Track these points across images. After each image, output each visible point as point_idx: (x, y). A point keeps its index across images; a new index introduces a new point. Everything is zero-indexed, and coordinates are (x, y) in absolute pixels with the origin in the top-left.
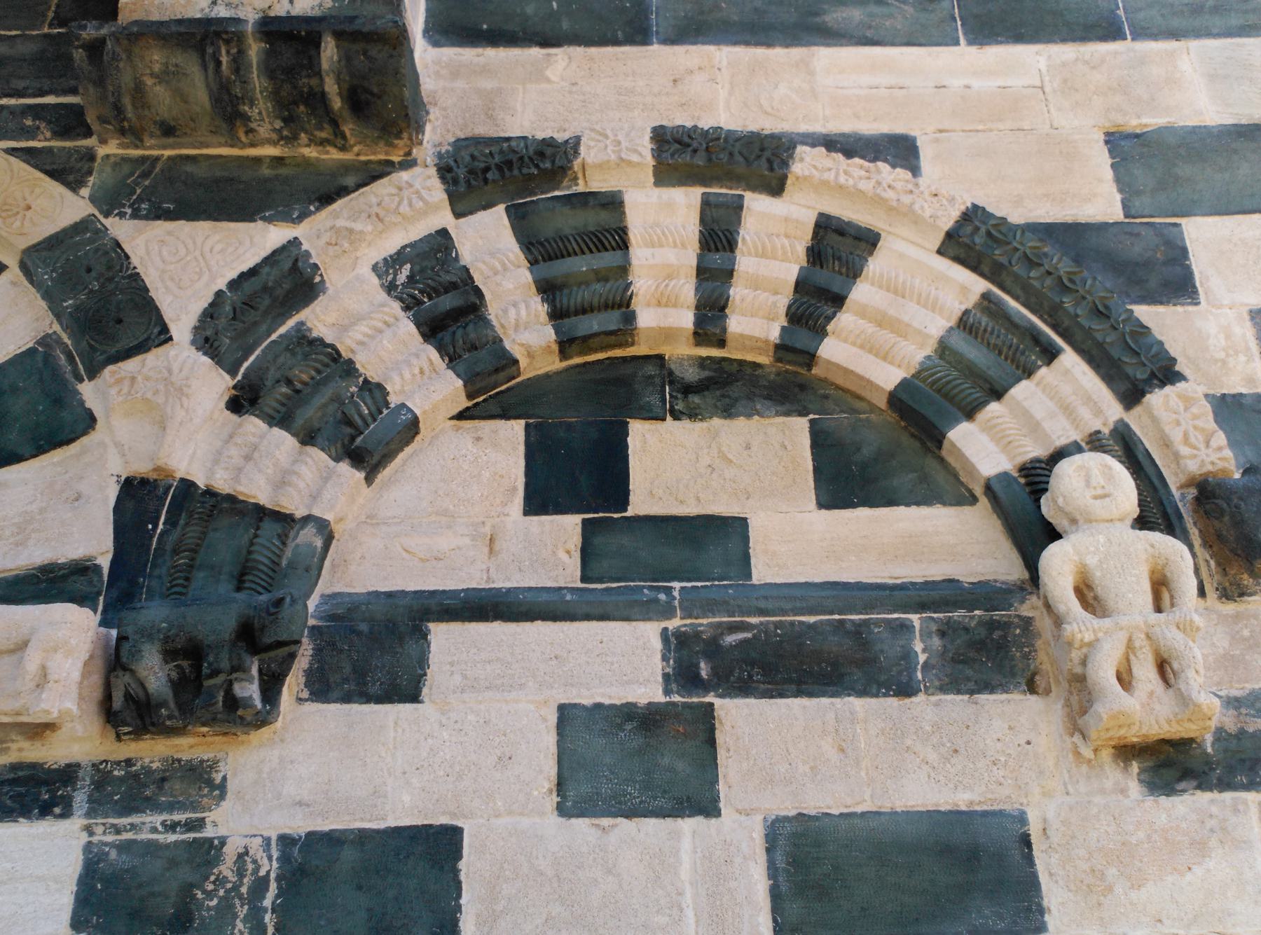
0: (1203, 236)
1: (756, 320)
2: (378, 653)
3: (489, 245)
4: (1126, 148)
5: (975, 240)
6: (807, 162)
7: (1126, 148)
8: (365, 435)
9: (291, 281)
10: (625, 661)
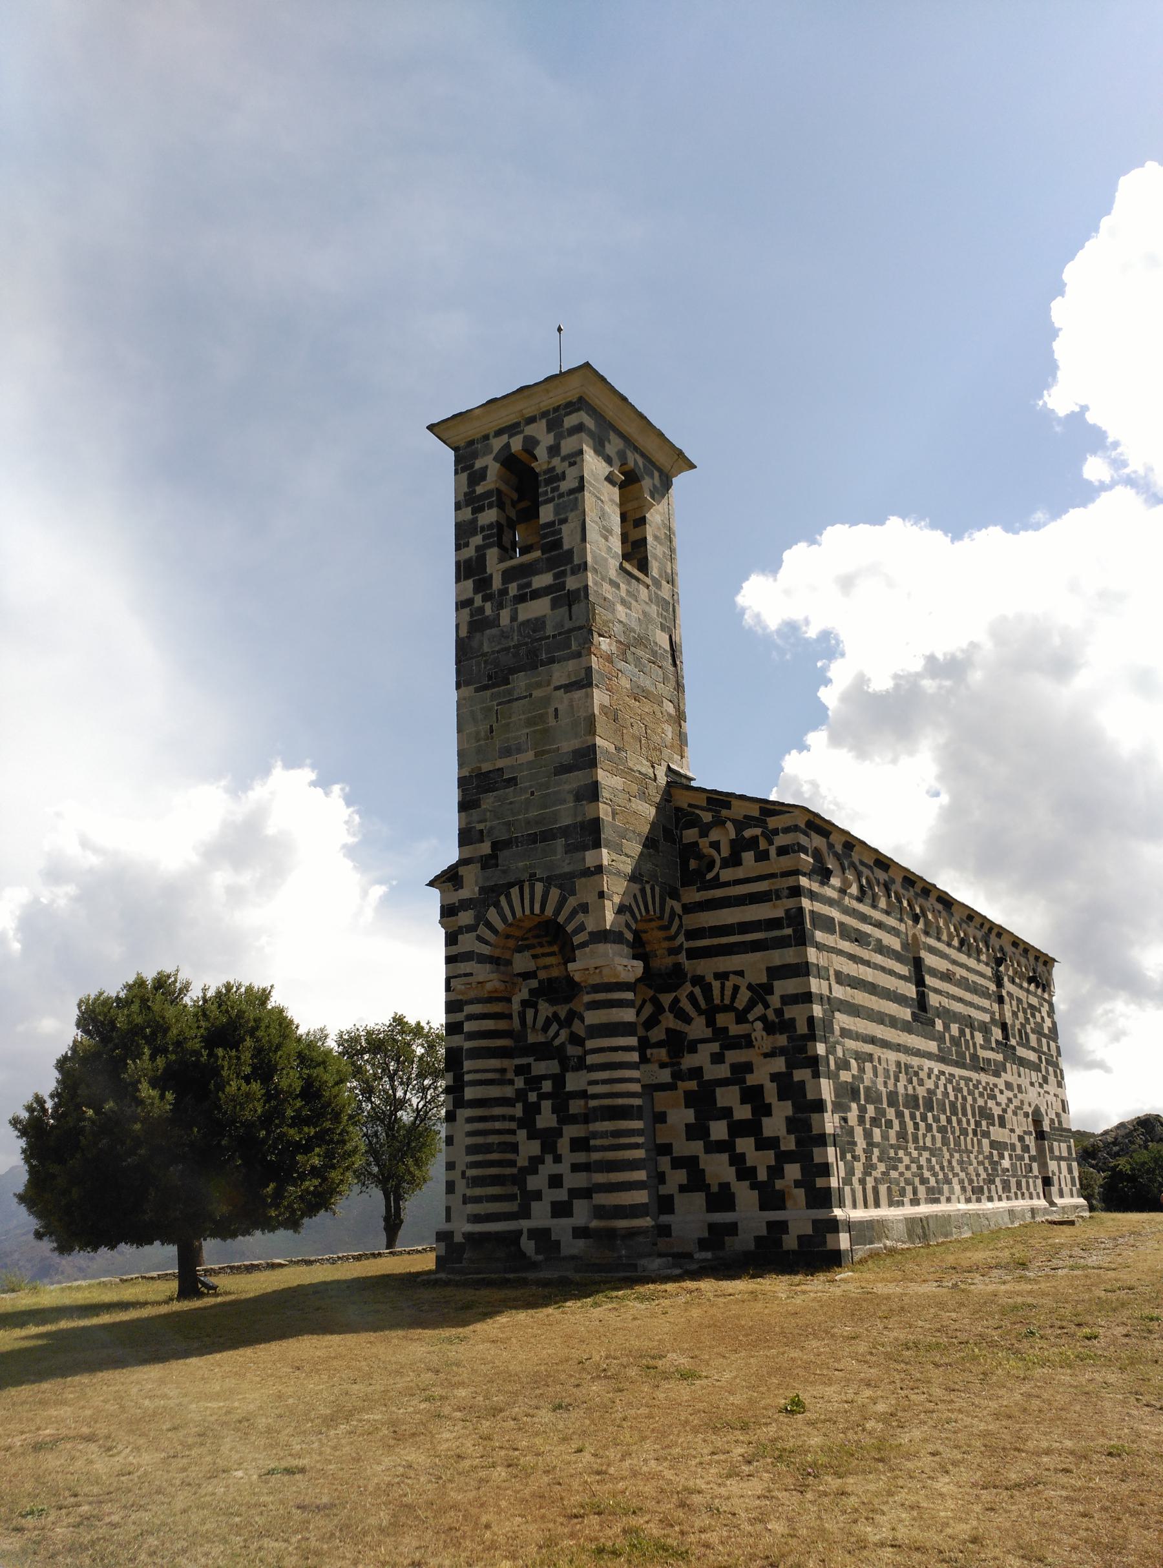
0: (776, 983)
1: (727, 1001)
2: (693, 1048)
3: (697, 991)
4: (769, 969)
5: (750, 987)
6: (732, 977)
7: (769, 969)
8: (688, 1020)
9: (676, 1000)
10: (715, 1047)
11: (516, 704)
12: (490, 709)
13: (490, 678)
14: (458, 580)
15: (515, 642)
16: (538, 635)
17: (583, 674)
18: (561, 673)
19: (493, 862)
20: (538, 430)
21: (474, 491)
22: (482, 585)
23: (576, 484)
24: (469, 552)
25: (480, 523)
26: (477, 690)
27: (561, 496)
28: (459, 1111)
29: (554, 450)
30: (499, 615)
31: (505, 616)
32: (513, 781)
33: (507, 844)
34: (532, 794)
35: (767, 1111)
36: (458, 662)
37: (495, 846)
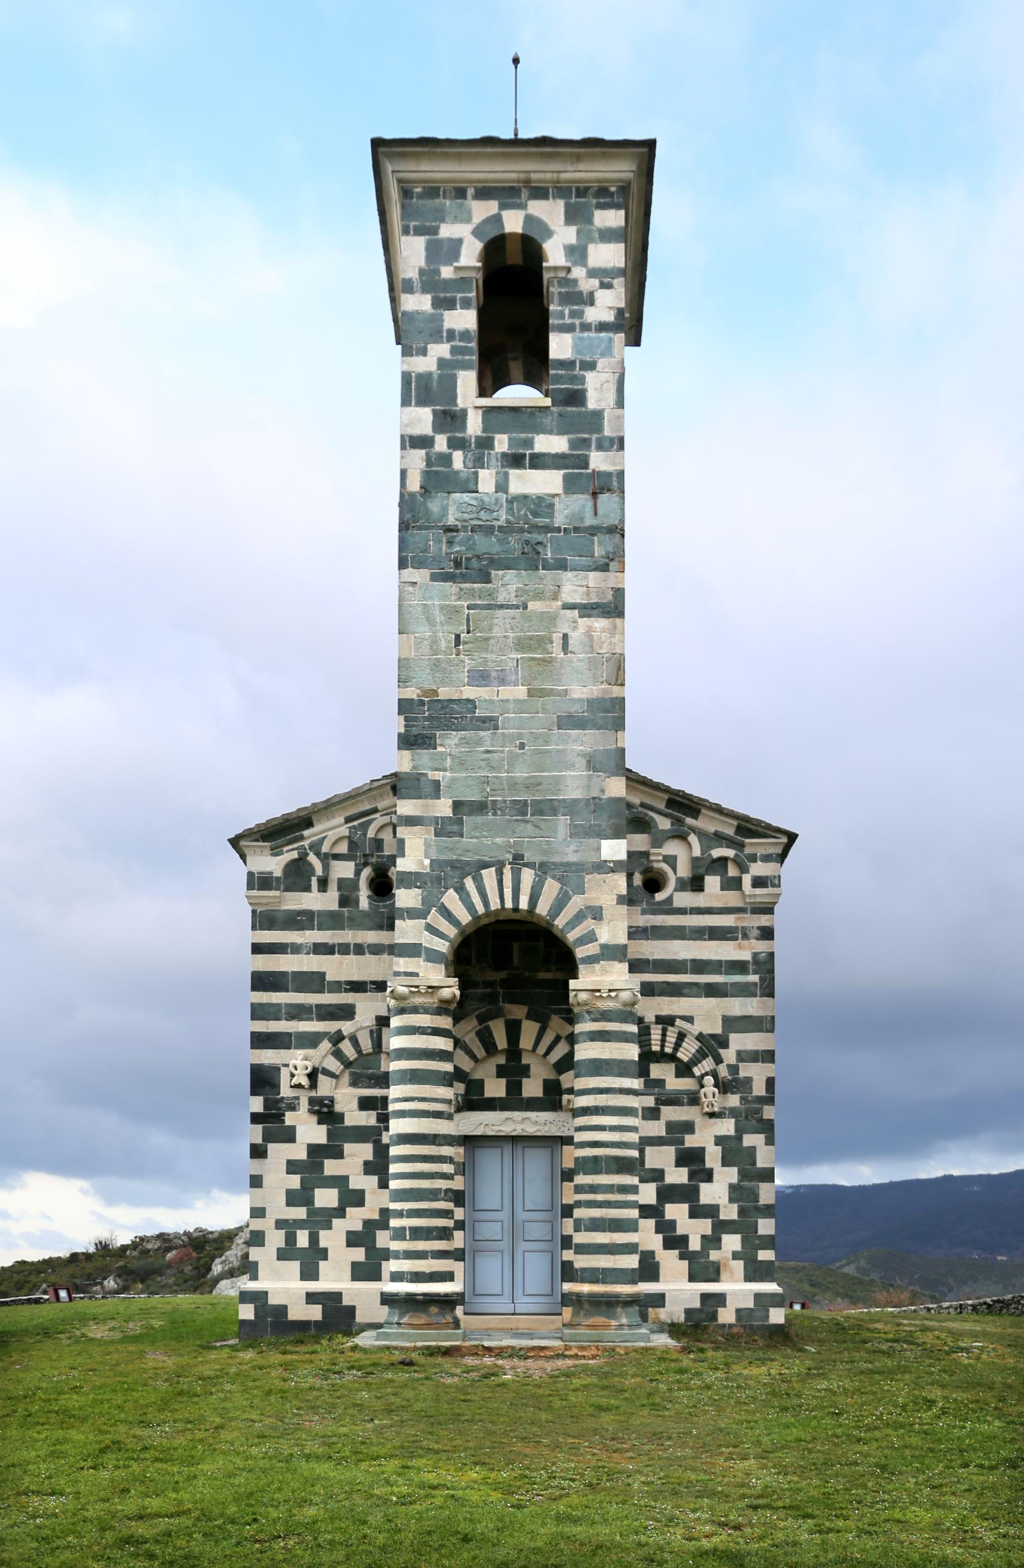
11: (500, 613)
12: (457, 611)
13: (457, 564)
14: (405, 402)
15: (502, 522)
16: (541, 521)
17: (609, 596)
18: (575, 586)
19: (455, 828)
20: (550, 212)
21: (438, 272)
22: (450, 419)
23: (609, 317)
24: (426, 364)
25: (447, 325)
26: (434, 578)
27: (586, 327)
28: (271, 1147)
29: (577, 253)
30: (476, 474)
31: (487, 480)
32: (489, 723)
33: (480, 807)
34: (522, 746)
35: (708, 1176)
36: (404, 526)
37: (457, 805)
